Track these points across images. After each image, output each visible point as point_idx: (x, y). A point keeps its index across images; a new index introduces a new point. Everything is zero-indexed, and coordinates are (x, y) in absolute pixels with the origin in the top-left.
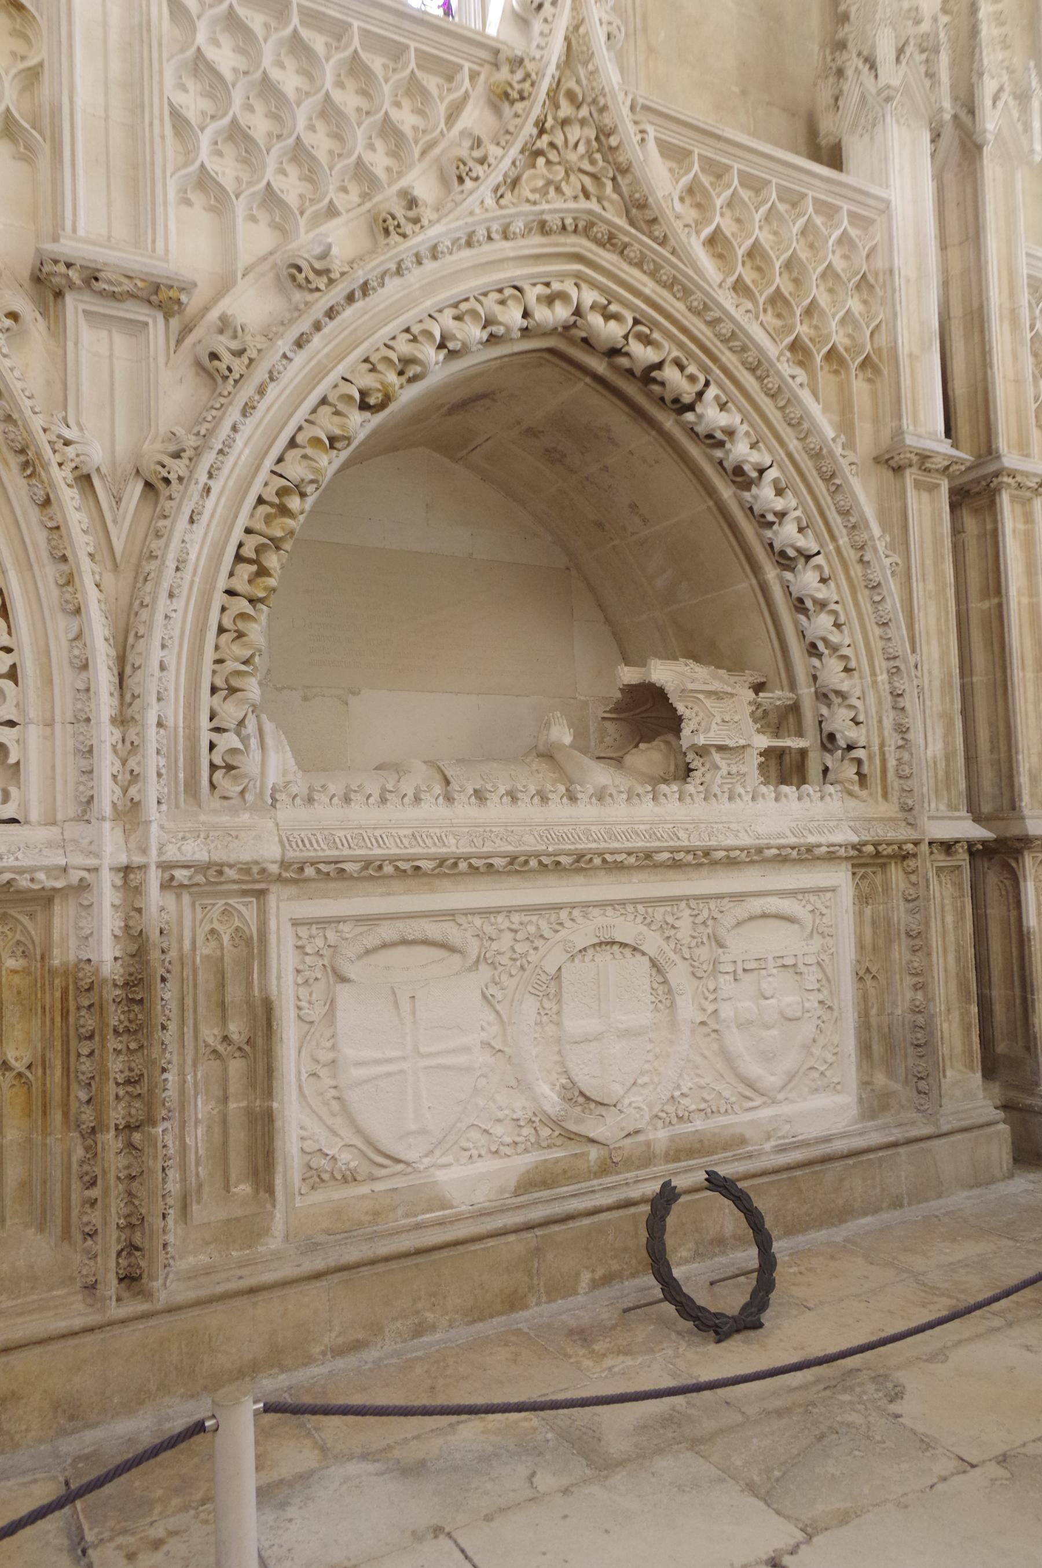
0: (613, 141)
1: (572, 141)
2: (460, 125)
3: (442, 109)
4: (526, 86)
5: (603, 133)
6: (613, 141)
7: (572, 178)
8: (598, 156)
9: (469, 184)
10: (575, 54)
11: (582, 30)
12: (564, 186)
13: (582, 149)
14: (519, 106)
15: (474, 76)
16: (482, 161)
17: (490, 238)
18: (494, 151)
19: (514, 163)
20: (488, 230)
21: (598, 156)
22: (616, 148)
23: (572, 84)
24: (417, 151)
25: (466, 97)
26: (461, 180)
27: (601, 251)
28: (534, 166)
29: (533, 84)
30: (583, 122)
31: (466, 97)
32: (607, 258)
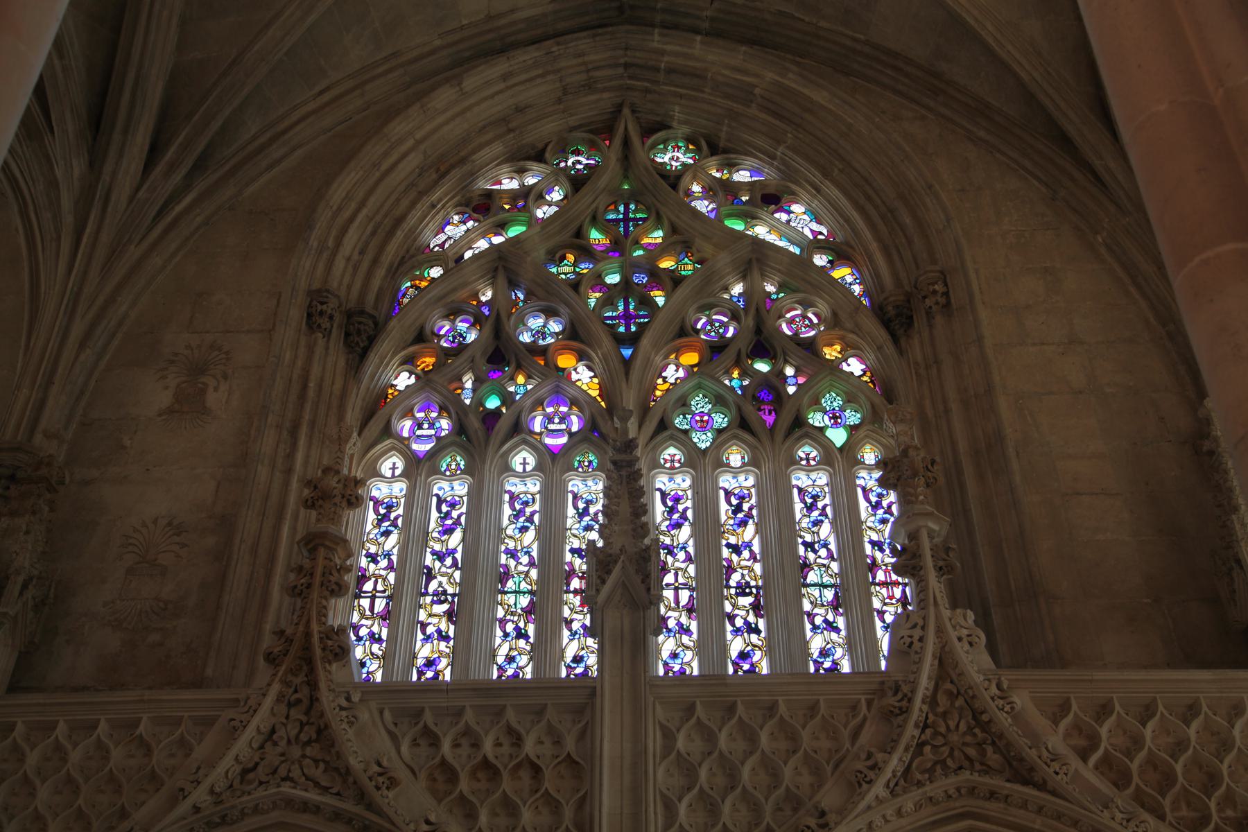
0: (985, 718)
1: (952, 724)
2: (857, 745)
3: (846, 734)
4: (904, 703)
5: (976, 715)
6: (985, 718)
7: (956, 753)
8: (977, 731)
9: (865, 786)
10: (944, 661)
11: (947, 649)
12: (949, 762)
13: (963, 727)
14: (901, 718)
15: (869, 703)
16: (872, 768)
17: (887, 821)
18: (880, 756)
19: (900, 759)
20: (884, 817)
21: (977, 731)
22: (990, 721)
23: (948, 686)
24: (829, 769)
25: (865, 719)
26: (860, 785)
27: (987, 804)
28: (921, 754)
29: (910, 700)
30: (961, 709)
31: (865, 719)
32: (993, 808)
